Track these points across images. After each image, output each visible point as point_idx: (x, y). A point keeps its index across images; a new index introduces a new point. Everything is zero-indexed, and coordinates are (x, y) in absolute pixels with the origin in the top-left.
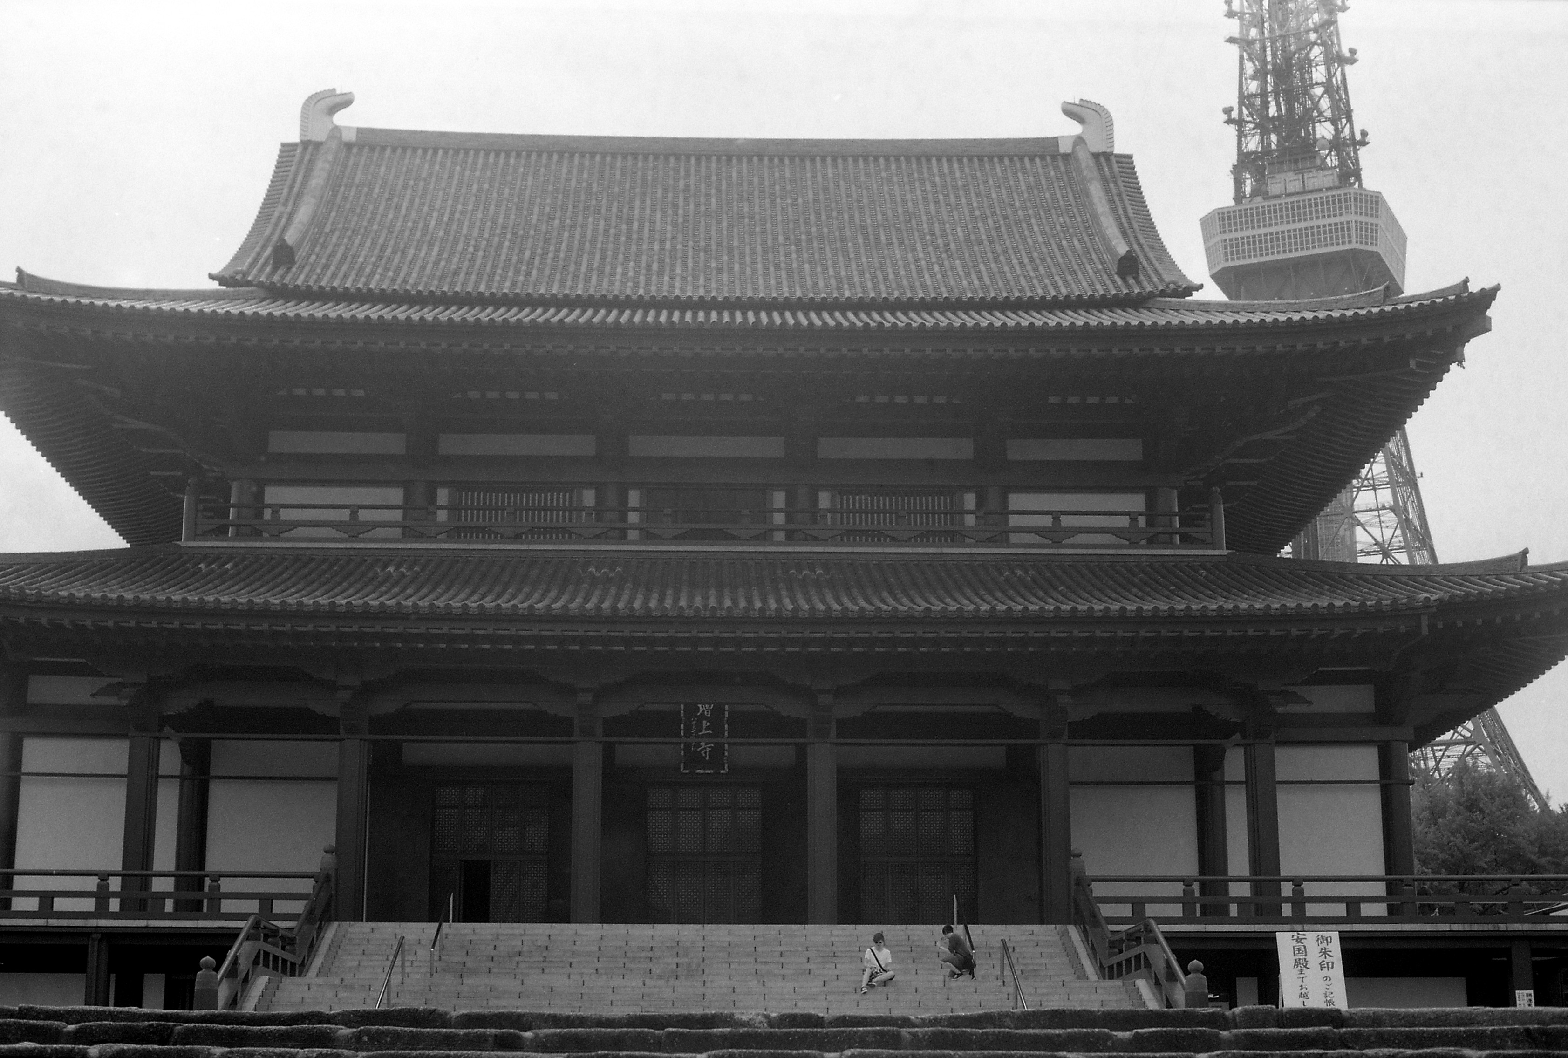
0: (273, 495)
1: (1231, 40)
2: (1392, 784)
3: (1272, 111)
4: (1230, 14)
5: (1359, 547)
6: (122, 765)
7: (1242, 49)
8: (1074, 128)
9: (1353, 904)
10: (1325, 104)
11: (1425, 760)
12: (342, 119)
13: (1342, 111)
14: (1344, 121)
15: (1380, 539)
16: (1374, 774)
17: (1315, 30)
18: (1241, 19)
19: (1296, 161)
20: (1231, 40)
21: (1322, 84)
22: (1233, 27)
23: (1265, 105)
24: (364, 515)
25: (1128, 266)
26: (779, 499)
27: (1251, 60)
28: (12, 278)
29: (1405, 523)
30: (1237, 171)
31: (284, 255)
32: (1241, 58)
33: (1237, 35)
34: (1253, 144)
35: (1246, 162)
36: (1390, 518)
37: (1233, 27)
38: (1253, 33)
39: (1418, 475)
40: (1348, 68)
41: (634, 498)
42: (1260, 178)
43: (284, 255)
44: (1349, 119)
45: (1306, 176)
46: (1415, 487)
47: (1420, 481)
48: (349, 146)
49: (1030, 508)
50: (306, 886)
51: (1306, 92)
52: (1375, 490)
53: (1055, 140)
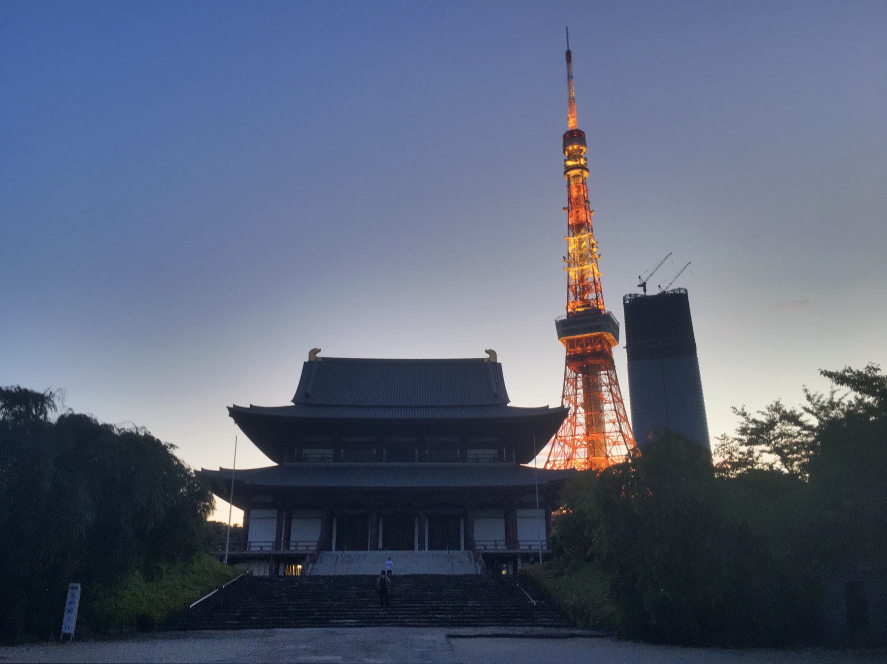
0: (305, 451)
2: (548, 517)
6: (276, 516)
8: (487, 356)
9: (530, 546)
10: (593, 287)
12: (319, 355)
16: (544, 515)
24: (326, 456)
25: (496, 396)
26: (417, 451)
28: (249, 406)
31: (307, 395)
41: (385, 452)
43: (307, 395)
48: (320, 362)
49: (472, 453)
50: (316, 543)
53: (483, 359)
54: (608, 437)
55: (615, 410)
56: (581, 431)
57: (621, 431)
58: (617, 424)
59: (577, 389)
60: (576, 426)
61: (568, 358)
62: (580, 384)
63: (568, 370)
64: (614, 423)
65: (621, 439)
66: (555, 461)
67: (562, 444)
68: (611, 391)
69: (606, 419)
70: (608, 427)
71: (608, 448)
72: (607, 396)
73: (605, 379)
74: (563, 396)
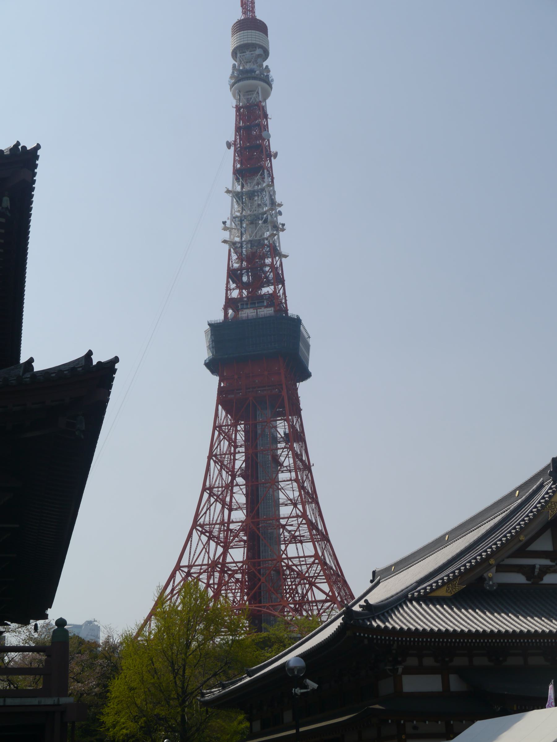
1: (225, 242)
3: (245, 279)
4: (225, 229)
5: (281, 501)
7: (230, 246)
10: (271, 276)
11: (312, 610)
13: (280, 280)
14: (280, 286)
15: (291, 497)
17: (267, 239)
18: (230, 232)
19: (255, 303)
20: (225, 242)
21: (268, 265)
22: (226, 235)
23: (241, 275)
27: (236, 253)
29: (301, 488)
30: (226, 309)
32: (230, 251)
33: (228, 239)
34: (235, 294)
35: (230, 303)
36: (295, 484)
37: (226, 235)
38: (237, 239)
39: (312, 465)
40: (284, 260)
42: (236, 310)
44: (283, 285)
45: (258, 310)
46: (310, 471)
47: (312, 468)
51: (262, 270)
52: (290, 472)
54: (284, 527)
55: (296, 480)
56: (239, 515)
57: (304, 515)
58: (300, 507)
59: (236, 447)
60: (230, 510)
61: (221, 391)
62: (240, 438)
63: (222, 413)
64: (295, 505)
65: (304, 531)
66: (190, 567)
67: (204, 539)
68: (291, 448)
69: (282, 497)
70: (285, 511)
71: (283, 547)
72: (288, 461)
73: (282, 428)
74: (210, 458)
